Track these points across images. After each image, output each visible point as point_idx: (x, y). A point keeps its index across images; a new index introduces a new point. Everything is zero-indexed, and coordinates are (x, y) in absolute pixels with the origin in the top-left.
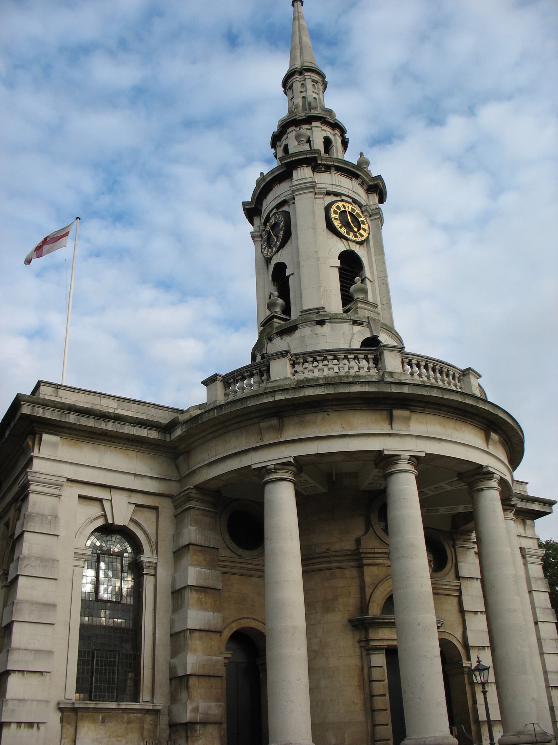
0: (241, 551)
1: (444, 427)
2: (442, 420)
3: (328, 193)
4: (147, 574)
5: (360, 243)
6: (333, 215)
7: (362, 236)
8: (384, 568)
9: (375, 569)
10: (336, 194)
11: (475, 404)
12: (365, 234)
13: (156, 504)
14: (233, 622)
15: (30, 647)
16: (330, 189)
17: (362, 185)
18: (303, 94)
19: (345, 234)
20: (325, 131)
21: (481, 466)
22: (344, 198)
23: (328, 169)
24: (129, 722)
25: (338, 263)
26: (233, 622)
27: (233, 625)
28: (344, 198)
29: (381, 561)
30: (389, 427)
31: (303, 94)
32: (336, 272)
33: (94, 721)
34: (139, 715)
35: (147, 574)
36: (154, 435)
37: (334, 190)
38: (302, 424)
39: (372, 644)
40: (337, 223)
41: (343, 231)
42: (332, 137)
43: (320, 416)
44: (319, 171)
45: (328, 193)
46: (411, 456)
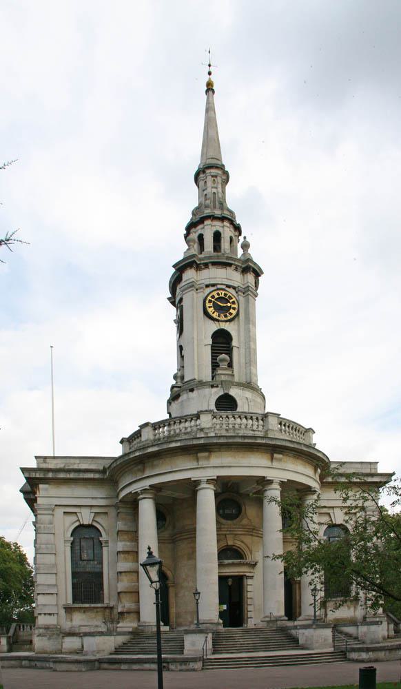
3: (207, 286)
5: (230, 321)
6: (208, 305)
7: (231, 314)
10: (213, 285)
12: (234, 312)
17: (236, 269)
19: (217, 318)
21: (264, 477)
23: (206, 265)
25: (210, 341)
28: (219, 286)
32: (209, 348)
40: (210, 310)
41: (215, 315)
45: (207, 286)
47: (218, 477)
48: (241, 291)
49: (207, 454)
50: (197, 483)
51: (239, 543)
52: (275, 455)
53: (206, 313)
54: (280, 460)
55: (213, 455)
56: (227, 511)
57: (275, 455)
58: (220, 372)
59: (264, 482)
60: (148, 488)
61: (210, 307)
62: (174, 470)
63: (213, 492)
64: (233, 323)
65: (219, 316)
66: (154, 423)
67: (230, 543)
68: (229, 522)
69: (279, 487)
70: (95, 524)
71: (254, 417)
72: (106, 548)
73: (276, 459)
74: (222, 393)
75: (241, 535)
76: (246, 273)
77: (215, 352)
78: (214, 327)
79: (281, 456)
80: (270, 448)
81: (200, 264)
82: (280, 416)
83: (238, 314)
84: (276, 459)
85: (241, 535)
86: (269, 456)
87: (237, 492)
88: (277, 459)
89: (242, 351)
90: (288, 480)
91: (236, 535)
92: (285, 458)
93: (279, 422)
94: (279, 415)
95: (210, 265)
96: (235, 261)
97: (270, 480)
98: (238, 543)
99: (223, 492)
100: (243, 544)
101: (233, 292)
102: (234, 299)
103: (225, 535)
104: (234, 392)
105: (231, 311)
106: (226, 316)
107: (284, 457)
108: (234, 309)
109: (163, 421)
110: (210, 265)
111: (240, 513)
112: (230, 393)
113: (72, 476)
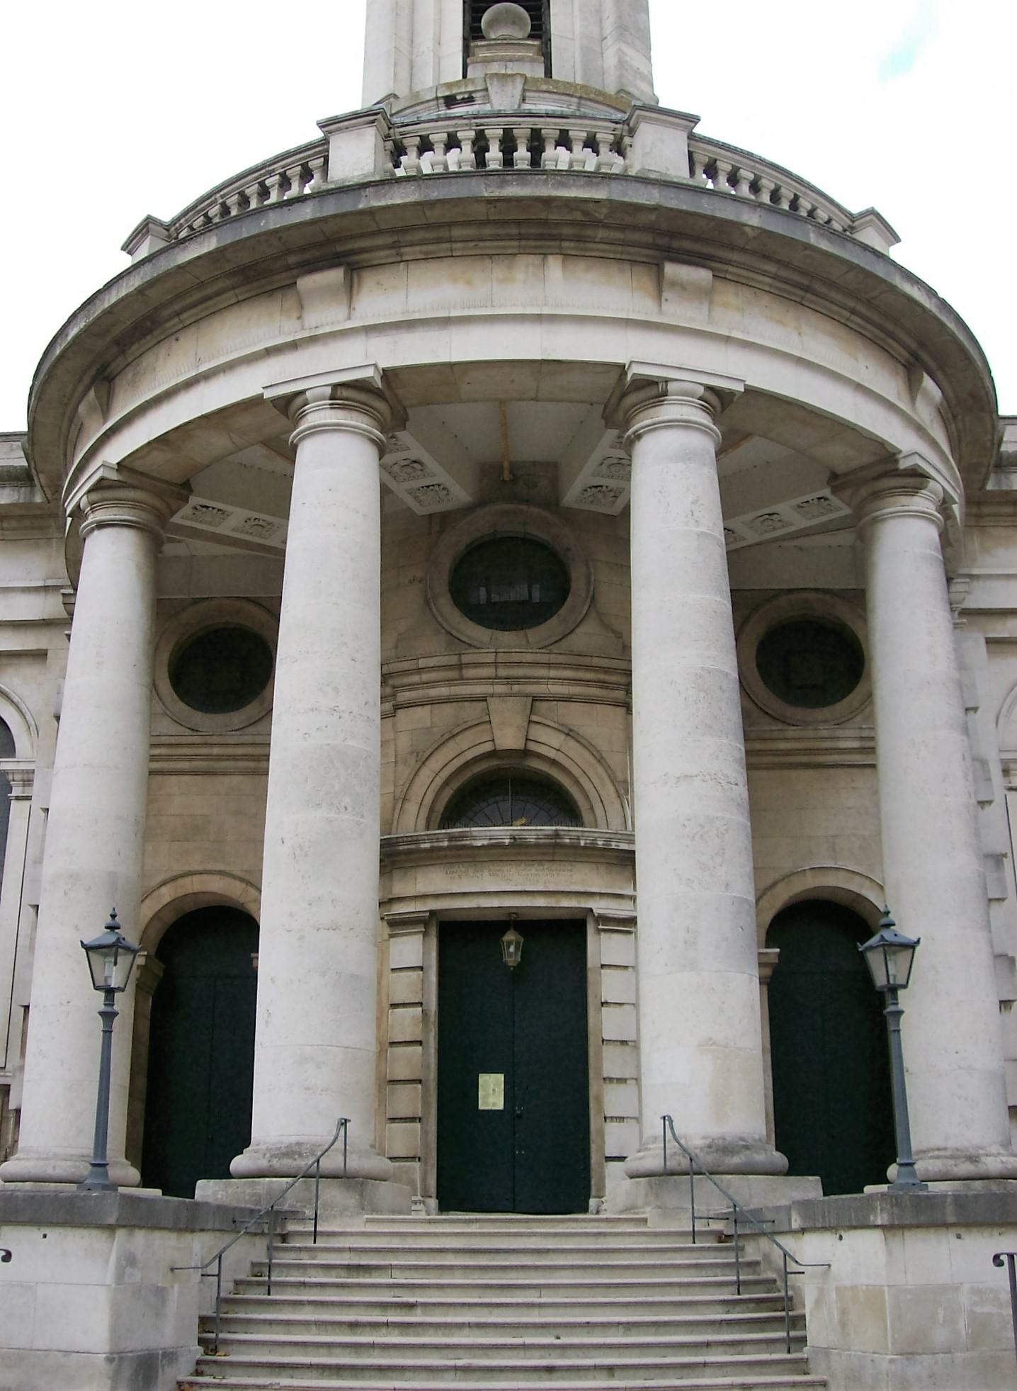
0: (198, 718)
1: (469, 283)
2: (459, 267)
4: (17, 798)
8: (448, 709)
9: (422, 714)
11: (497, 193)
14: (164, 883)
21: (621, 369)
26: (164, 883)
27: (164, 890)
29: (444, 691)
30: (297, 324)
35: (17, 798)
38: (134, 384)
43: (163, 350)
46: (335, 386)
47: (387, 374)
49: (335, 276)
51: (555, 739)
52: (671, 269)
54: (705, 294)
55: (369, 281)
56: (519, 592)
58: (483, 54)
59: (623, 399)
60: (113, 476)
62: (204, 368)
63: (370, 452)
66: (174, 222)
67: (509, 739)
68: (507, 638)
69: (704, 419)
71: (578, 135)
72: (26, 804)
73: (673, 284)
75: (568, 699)
79: (702, 275)
80: (647, 238)
82: (699, 130)
84: (673, 284)
85: (568, 699)
86: (647, 281)
87: (552, 503)
88: (680, 287)
91: (536, 699)
92: (730, 296)
93: (701, 159)
94: (694, 120)
97: (650, 382)
98: (549, 742)
99: (481, 503)
100: (572, 747)
103: (483, 699)
107: (720, 285)
109: (202, 200)
111: (564, 599)
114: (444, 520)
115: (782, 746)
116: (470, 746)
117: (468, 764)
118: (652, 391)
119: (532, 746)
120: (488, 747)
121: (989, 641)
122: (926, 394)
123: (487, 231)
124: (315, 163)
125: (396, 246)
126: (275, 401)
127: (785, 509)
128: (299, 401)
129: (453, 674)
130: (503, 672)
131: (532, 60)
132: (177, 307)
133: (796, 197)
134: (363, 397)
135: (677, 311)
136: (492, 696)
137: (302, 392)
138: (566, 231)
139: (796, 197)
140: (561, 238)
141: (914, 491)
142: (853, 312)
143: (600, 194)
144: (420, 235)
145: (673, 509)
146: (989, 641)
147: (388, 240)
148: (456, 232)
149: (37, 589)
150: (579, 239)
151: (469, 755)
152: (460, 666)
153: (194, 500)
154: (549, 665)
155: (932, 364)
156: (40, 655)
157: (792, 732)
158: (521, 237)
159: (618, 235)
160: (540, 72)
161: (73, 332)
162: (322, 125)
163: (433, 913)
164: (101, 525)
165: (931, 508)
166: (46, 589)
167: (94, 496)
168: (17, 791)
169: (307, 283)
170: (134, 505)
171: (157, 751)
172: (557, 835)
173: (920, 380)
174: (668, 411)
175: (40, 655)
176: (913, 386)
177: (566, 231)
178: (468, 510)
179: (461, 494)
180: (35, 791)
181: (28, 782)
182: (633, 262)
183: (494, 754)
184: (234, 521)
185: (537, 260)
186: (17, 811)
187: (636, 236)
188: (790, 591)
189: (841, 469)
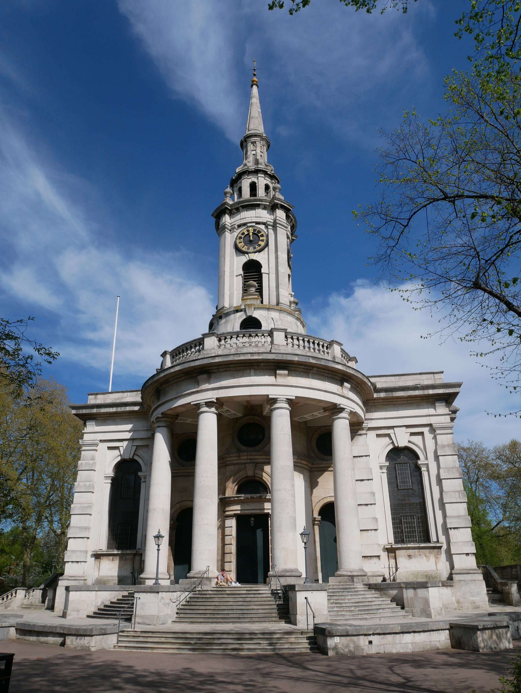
3: (239, 226)
5: (260, 251)
6: (238, 241)
7: (259, 245)
10: (244, 224)
12: (262, 244)
13: (148, 444)
14: (177, 503)
15: (78, 526)
16: (239, 223)
17: (265, 208)
18: (254, 152)
19: (246, 250)
20: (250, 178)
21: (268, 396)
22: (249, 225)
24: (126, 560)
25: (242, 272)
26: (177, 503)
28: (249, 225)
29: (236, 462)
31: (254, 152)
32: (240, 279)
33: (109, 560)
34: (131, 556)
36: (137, 408)
37: (242, 222)
39: (227, 513)
40: (240, 245)
41: (244, 249)
42: (255, 180)
44: (234, 214)
45: (239, 226)
46: (206, 402)
47: (217, 399)
48: (270, 225)
49: (205, 376)
50: (198, 406)
52: (278, 372)
53: (239, 251)
57: (278, 372)
60: (160, 416)
61: (240, 243)
64: (263, 252)
65: (248, 249)
67: (250, 473)
69: (287, 406)
70: (136, 458)
72: (145, 483)
74: (245, 317)
76: (275, 210)
77: (246, 279)
78: (244, 259)
79: (286, 372)
81: (232, 209)
83: (267, 245)
88: (281, 375)
89: (273, 276)
90: (296, 397)
91: (256, 463)
95: (241, 208)
96: (261, 201)
99: (245, 416)
101: (262, 227)
102: (262, 233)
103: (245, 464)
104: (257, 314)
105: (260, 243)
106: (255, 248)
108: (262, 241)
109: (178, 348)
110: (241, 208)
112: (253, 316)
113: (114, 410)
114: (237, 420)
115: (322, 466)
116: (242, 475)
117: (242, 479)
118: (273, 401)
119: (256, 475)
120: (246, 475)
121: (377, 435)
122: (346, 387)
123: (237, 365)
124: (201, 342)
125: (218, 369)
126: (194, 405)
127: (315, 413)
128: (198, 405)
129: (238, 458)
130: (249, 457)
131: (257, 299)
132: (173, 379)
133: (314, 341)
134: (212, 404)
135: (280, 380)
136: (247, 463)
137: (199, 403)
138: (255, 364)
139: (314, 341)
140: (254, 366)
141: (341, 412)
142: (324, 372)
143: (261, 357)
144: (223, 367)
145: (281, 426)
146: (377, 435)
147: (216, 368)
148: (231, 366)
149: (146, 430)
150: (258, 366)
151: (242, 477)
152: (239, 456)
153: (179, 418)
154: (259, 455)
155: (348, 379)
156: (147, 446)
157: (324, 462)
158: (244, 366)
159: (266, 364)
160: (259, 301)
161: (150, 382)
162: (203, 335)
163: (235, 514)
164: (159, 427)
165: (347, 416)
166: (148, 430)
167: (157, 420)
168: (143, 480)
169: (200, 377)
170: (166, 421)
171: (175, 471)
172: (261, 496)
173: (343, 384)
174: (277, 405)
175: (147, 446)
176: (342, 385)
177: (255, 364)
178: (240, 418)
179: (239, 415)
180: (147, 480)
181: (145, 478)
182: (270, 369)
183: (247, 477)
184: (189, 421)
185: (248, 371)
186: (143, 485)
187: (270, 364)
188: (324, 426)
189: (325, 407)
